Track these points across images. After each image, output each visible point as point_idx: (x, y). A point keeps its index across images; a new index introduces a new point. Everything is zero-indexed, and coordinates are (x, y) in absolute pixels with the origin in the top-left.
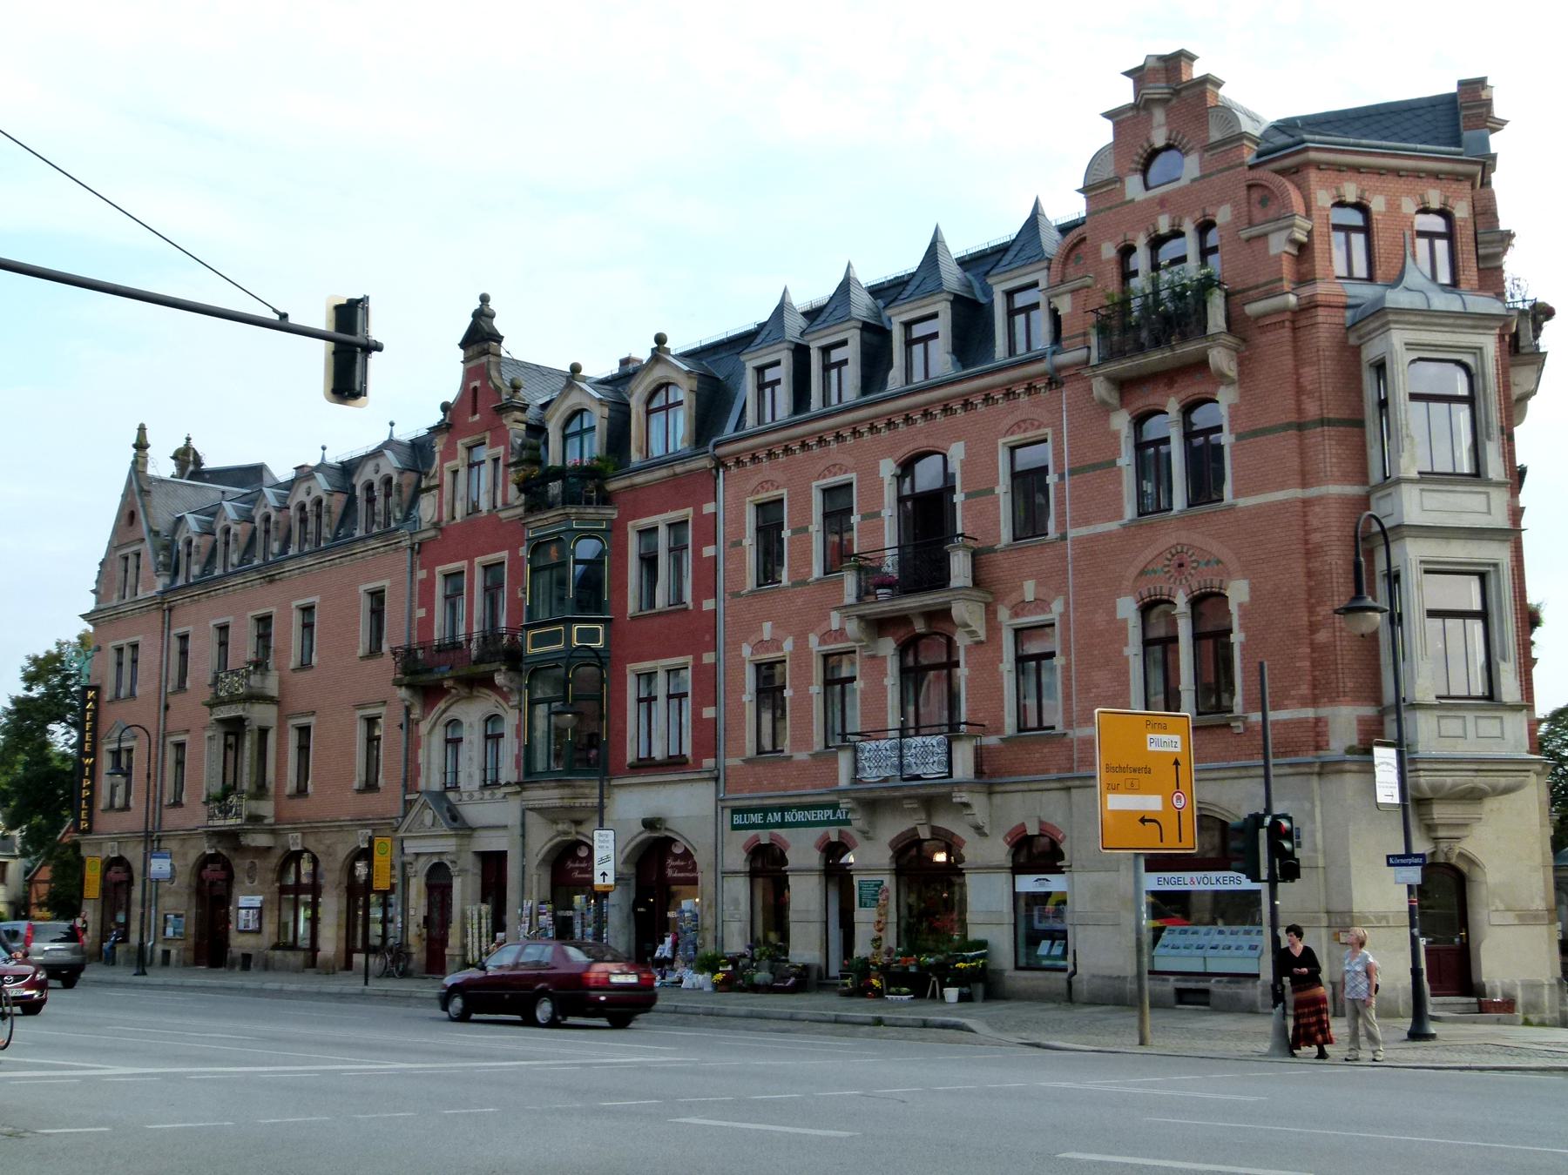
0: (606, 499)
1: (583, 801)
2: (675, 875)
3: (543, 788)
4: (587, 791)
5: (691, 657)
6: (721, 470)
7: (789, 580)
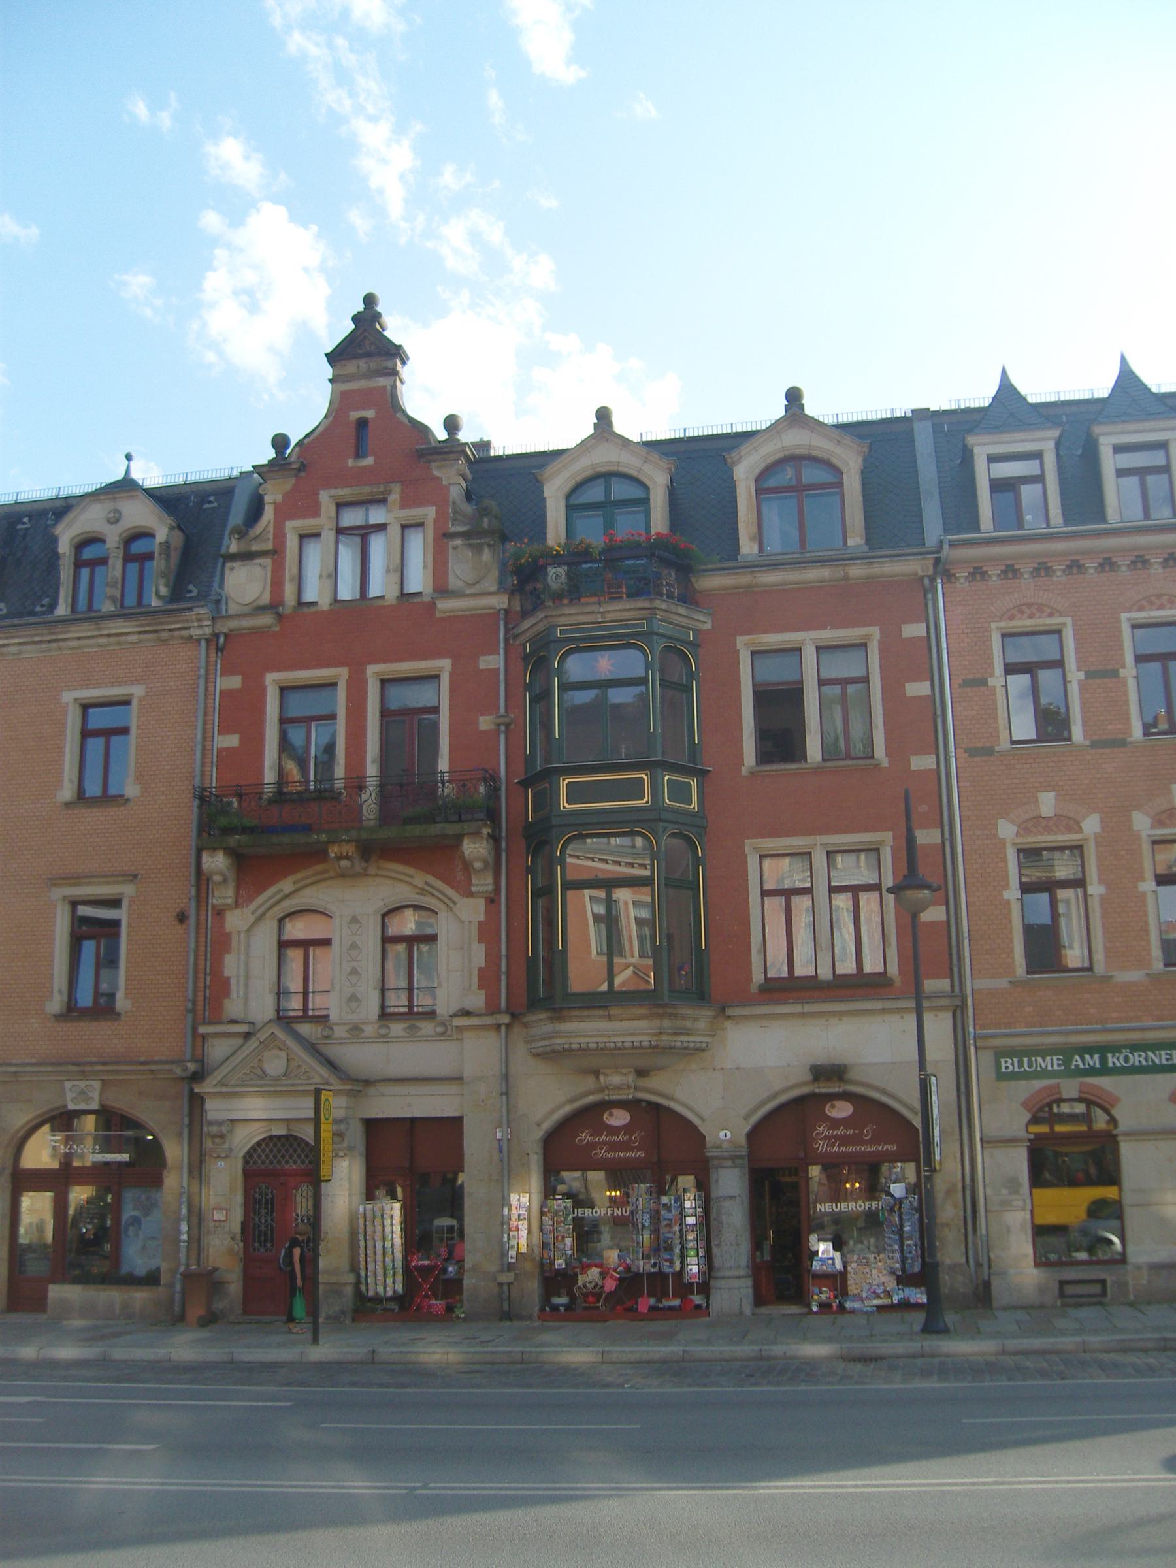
0: (689, 598)
1: (684, 1038)
2: (835, 1149)
3: (610, 1018)
4: (688, 1024)
5: (891, 834)
6: (939, 581)
7: (1085, 738)
